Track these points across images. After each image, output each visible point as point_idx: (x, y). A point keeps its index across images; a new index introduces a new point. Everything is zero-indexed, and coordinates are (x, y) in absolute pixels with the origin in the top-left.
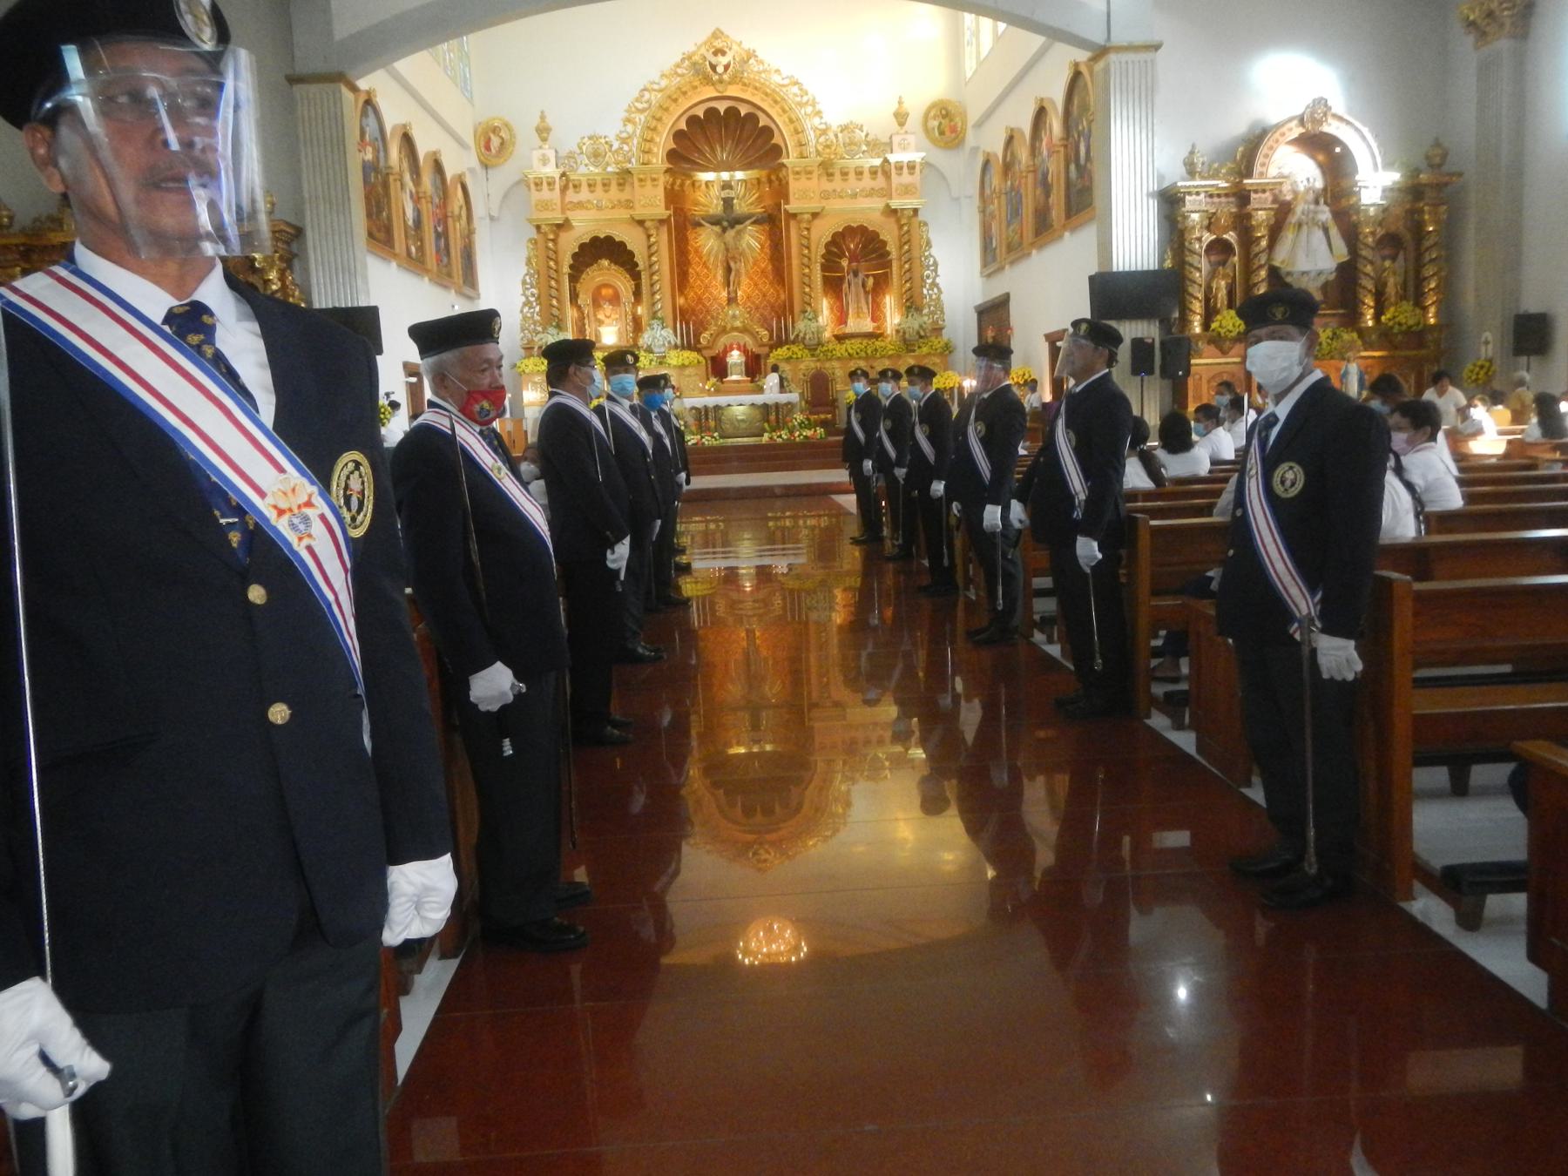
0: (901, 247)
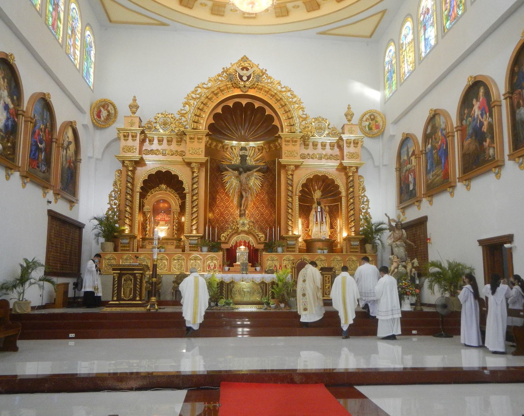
0: (347, 189)
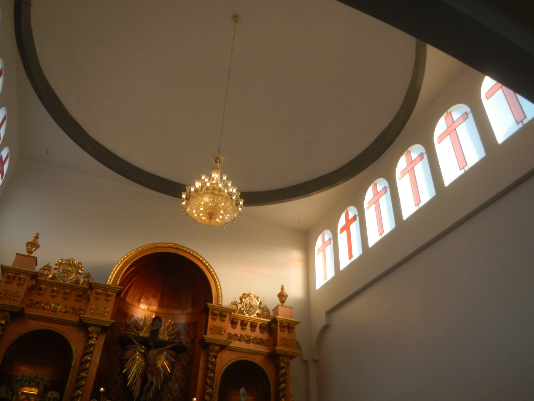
0: (278, 384)
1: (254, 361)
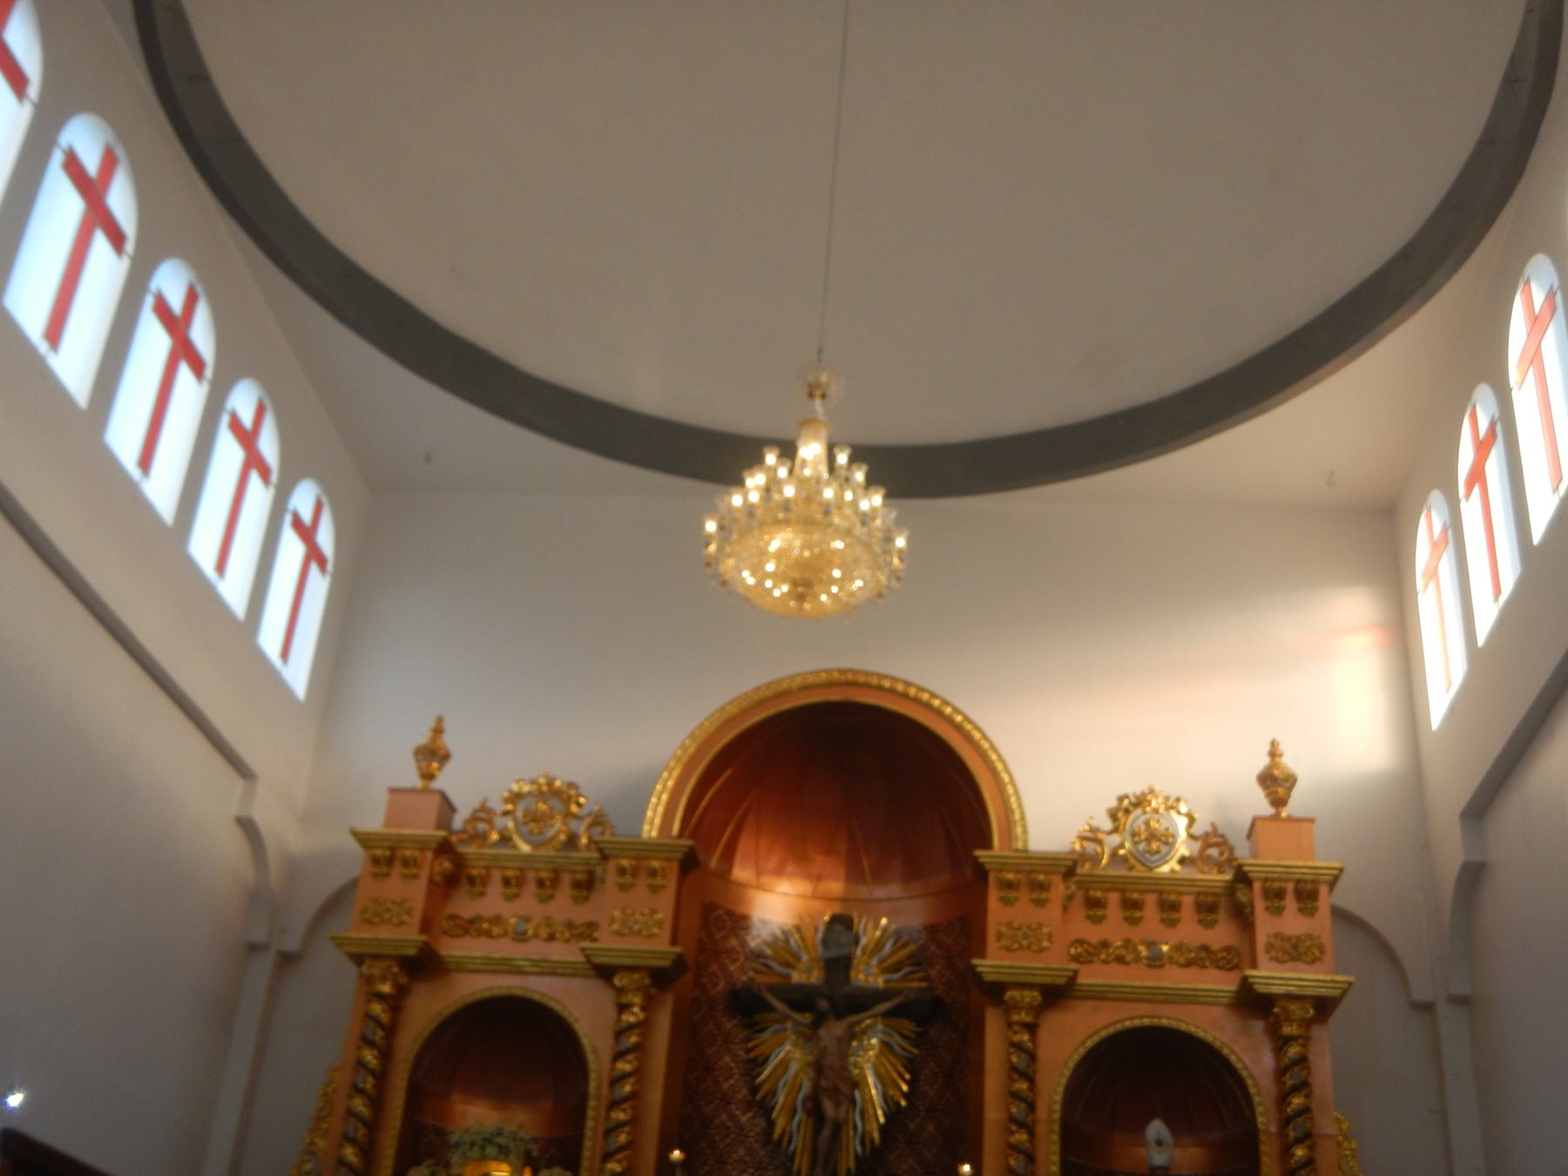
0: (1283, 1098)
1: (1183, 1027)
